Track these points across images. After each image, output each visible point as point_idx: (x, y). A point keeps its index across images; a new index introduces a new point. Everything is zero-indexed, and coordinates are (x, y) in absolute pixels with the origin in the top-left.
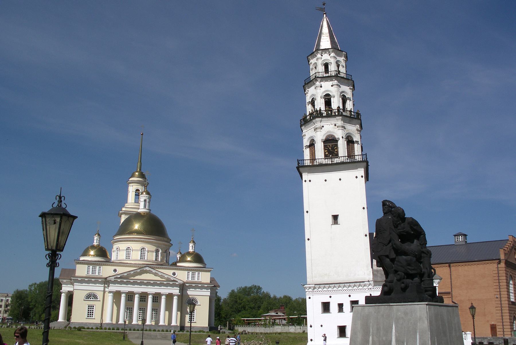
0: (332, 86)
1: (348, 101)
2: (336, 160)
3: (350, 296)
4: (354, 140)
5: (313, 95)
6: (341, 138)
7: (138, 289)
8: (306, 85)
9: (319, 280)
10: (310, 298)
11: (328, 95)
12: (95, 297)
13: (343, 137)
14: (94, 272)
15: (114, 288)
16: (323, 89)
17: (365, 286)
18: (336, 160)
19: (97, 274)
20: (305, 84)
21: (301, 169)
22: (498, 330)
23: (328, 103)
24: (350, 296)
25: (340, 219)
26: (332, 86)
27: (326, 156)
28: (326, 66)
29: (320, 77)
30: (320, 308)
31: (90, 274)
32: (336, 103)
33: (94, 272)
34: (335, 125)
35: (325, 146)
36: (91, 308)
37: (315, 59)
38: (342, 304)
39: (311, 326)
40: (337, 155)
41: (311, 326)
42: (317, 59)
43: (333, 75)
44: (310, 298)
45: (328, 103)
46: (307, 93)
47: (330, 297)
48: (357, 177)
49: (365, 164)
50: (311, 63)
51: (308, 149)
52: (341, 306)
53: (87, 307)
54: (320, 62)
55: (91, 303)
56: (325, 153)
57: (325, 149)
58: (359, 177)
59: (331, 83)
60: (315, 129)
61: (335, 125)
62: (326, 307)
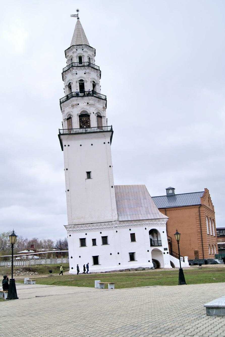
0: (85, 74)
1: (97, 86)
2: (89, 130)
3: (101, 233)
4: (102, 116)
5: (69, 80)
6: (92, 113)
8: (64, 73)
10: (70, 236)
11: (81, 80)
13: (93, 113)
16: (78, 76)
17: (112, 224)
18: (89, 130)
20: (63, 72)
21: (62, 137)
22: (199, 254)
23: (82, 86)
25: (92, 175)
26: (85, 74)
27: (81, 127)
28: (80, 58)
29: (76, 66)
30: (79, 243)
32: (88, 87)
34: (88, 103)
35: (80, 119)
37: (71, 52)
38: (134, 234)
39: (72, 257)
40: (89, 127)
41: (72, 257)
42: (73, 53)
43: (86, 65)
45: (82, 86)
46: (65, 79)
47: (86, 234)
48: (104, 143)
49: (111, 133)
50: (68, 56)
51: (66, 122)
52: (94, 241)
54: (75, 55)
56: (80, 124)
57: (80, 122)
59: (84, 71)
60: (73, 106)
61: (88, 103)
62: (83, 242)
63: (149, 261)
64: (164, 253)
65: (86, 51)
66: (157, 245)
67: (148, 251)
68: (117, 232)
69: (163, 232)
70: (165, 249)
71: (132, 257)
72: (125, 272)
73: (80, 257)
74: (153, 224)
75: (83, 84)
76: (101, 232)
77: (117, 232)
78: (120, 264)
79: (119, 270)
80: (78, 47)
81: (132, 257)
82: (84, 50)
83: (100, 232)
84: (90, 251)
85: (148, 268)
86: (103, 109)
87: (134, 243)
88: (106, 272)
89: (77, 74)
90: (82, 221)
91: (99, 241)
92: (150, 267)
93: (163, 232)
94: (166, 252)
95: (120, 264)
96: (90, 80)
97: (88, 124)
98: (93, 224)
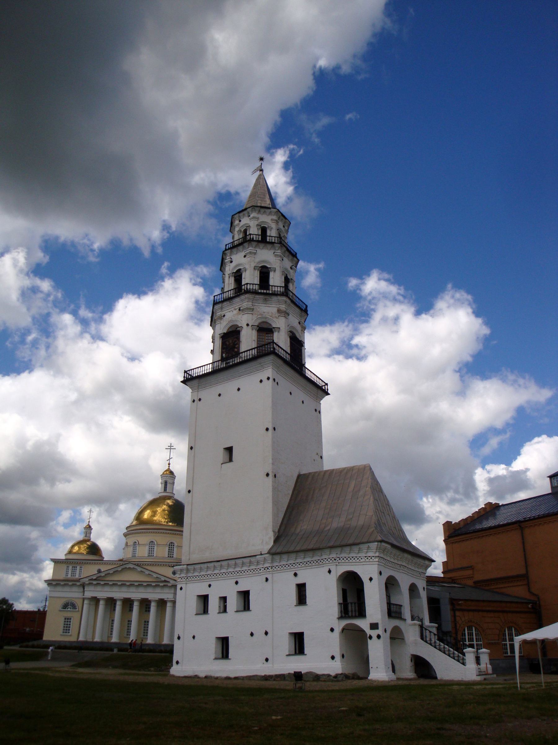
0: (245, 256)
1: (272, 274)
6: (245, 326)
7: (119, 594)
9: (196, 557)
10: (181, 589)
12: (74, 606)
14: (73, 573)
15: (90, 593)
17: (258, 563)
19: (69, 576)
24: (237, 583)
26: (245, 256)
30: (194, 604)
31: (69, 576)
33: (73, 573)
36: (68, 620)
44: (181, 589)
47: (210, 586)
53: (63, 620)
55: (68, 615)
58: (265, 379)
59: (243, 254)
63: (333, 658)
64: (371, 637)
65: (254, 218)
66: (357, 614)
67: (332, 630)
68: (267, 580)
69: (371, 579)
70: (374, 626)
71: (298, 642)
72: (274, 682)
73: (194, 637)
74: (349, 559)
75: (241, 276)
76: (238, 580)
77: (267, 580)
78: (267, 660)
79: (263, 674)
80: (241, 214)
81: (298, 642)
82: (251, 216)
83: (235, 580)
84: (216, 624)
85: (329, 675)
86: (277, 315)
87: (301, 608)
88: (236, 678)
89: (231, 262)
90: (207, 556)
91: (233, 603)
92: (333, 674)
93: (371, 579)
94: (374, 633)
95: (267, 660)
96: (253, 265)
97: (236, 350)
98: (221, 562)
